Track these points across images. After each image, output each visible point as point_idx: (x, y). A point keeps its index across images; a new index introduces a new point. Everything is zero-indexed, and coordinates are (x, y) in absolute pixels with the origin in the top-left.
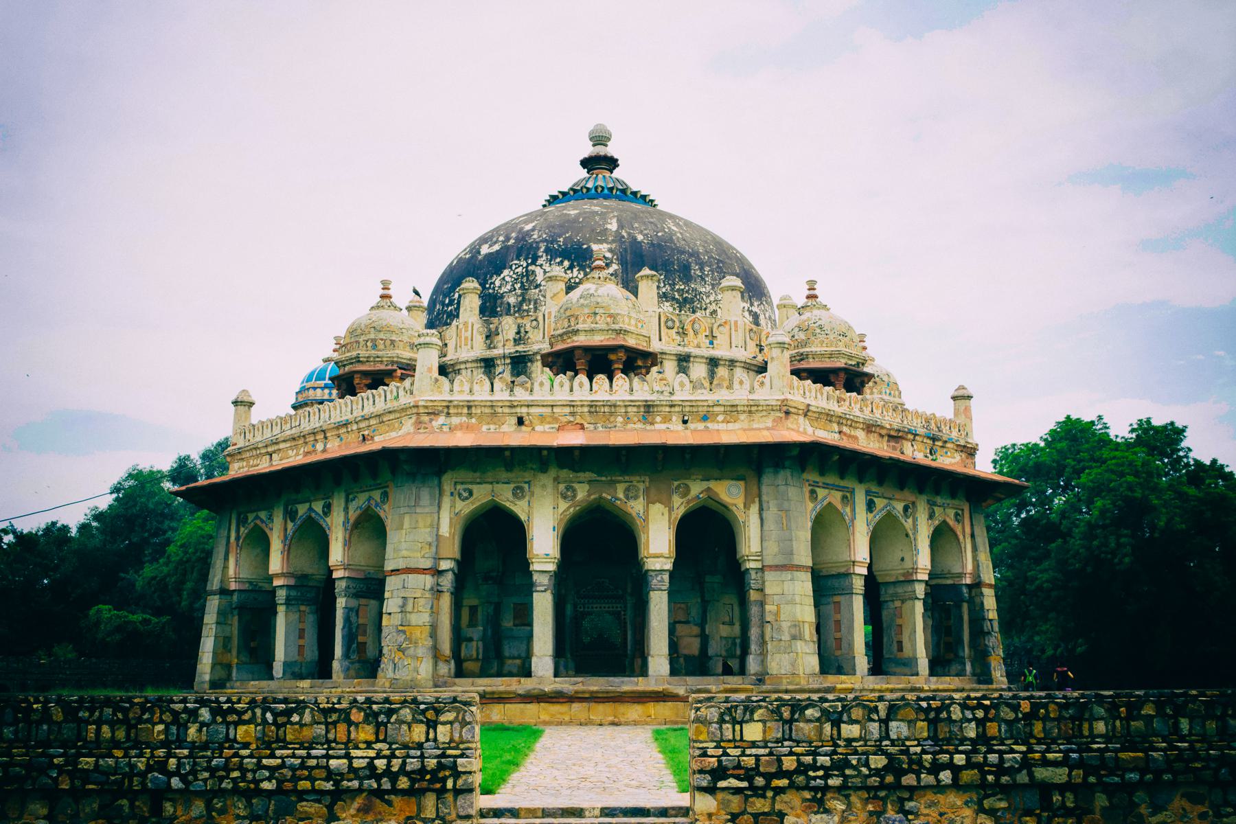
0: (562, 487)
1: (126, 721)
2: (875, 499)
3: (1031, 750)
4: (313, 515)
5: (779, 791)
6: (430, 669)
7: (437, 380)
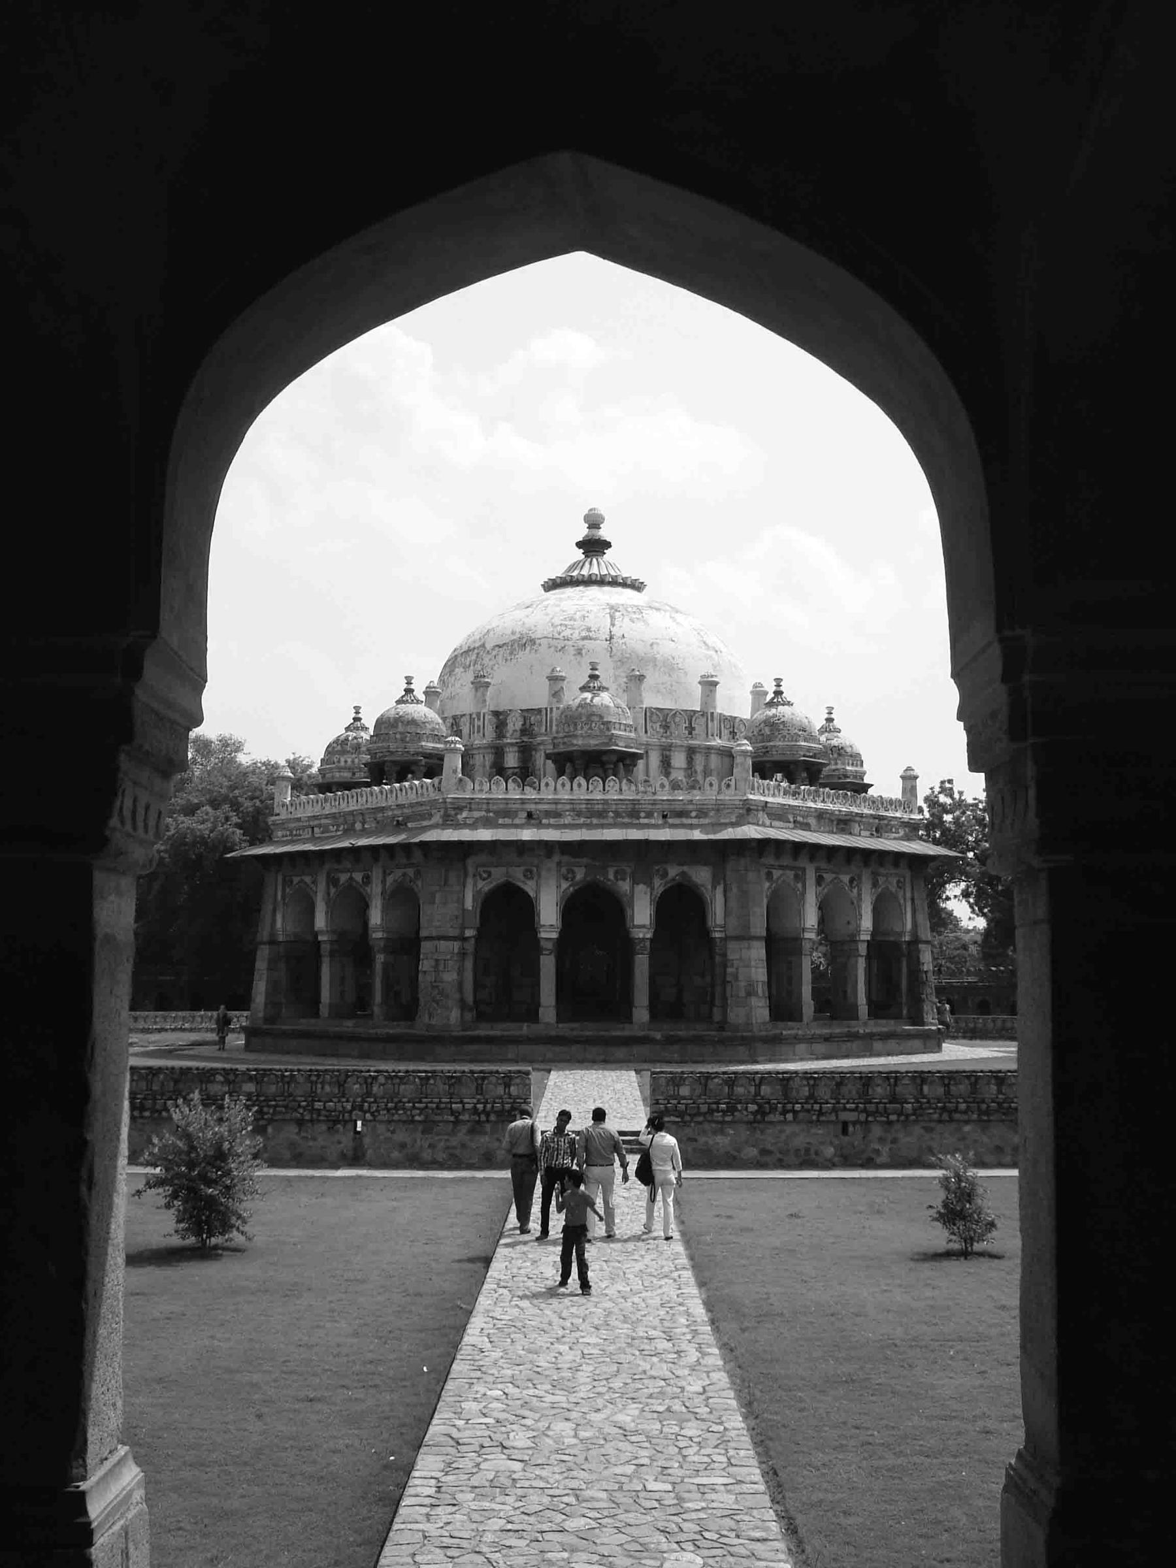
0: (564, 870)
1: (338, 1081)
2: (825, 875)
3: (838, 1103)
4: (354, 884)
5: (700, 1123)
6: (459, 1015)
7: (461, 780)
